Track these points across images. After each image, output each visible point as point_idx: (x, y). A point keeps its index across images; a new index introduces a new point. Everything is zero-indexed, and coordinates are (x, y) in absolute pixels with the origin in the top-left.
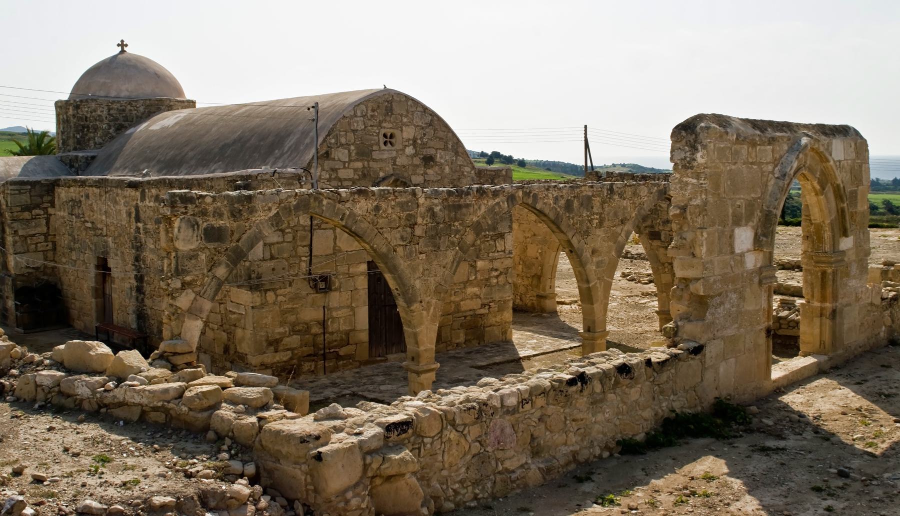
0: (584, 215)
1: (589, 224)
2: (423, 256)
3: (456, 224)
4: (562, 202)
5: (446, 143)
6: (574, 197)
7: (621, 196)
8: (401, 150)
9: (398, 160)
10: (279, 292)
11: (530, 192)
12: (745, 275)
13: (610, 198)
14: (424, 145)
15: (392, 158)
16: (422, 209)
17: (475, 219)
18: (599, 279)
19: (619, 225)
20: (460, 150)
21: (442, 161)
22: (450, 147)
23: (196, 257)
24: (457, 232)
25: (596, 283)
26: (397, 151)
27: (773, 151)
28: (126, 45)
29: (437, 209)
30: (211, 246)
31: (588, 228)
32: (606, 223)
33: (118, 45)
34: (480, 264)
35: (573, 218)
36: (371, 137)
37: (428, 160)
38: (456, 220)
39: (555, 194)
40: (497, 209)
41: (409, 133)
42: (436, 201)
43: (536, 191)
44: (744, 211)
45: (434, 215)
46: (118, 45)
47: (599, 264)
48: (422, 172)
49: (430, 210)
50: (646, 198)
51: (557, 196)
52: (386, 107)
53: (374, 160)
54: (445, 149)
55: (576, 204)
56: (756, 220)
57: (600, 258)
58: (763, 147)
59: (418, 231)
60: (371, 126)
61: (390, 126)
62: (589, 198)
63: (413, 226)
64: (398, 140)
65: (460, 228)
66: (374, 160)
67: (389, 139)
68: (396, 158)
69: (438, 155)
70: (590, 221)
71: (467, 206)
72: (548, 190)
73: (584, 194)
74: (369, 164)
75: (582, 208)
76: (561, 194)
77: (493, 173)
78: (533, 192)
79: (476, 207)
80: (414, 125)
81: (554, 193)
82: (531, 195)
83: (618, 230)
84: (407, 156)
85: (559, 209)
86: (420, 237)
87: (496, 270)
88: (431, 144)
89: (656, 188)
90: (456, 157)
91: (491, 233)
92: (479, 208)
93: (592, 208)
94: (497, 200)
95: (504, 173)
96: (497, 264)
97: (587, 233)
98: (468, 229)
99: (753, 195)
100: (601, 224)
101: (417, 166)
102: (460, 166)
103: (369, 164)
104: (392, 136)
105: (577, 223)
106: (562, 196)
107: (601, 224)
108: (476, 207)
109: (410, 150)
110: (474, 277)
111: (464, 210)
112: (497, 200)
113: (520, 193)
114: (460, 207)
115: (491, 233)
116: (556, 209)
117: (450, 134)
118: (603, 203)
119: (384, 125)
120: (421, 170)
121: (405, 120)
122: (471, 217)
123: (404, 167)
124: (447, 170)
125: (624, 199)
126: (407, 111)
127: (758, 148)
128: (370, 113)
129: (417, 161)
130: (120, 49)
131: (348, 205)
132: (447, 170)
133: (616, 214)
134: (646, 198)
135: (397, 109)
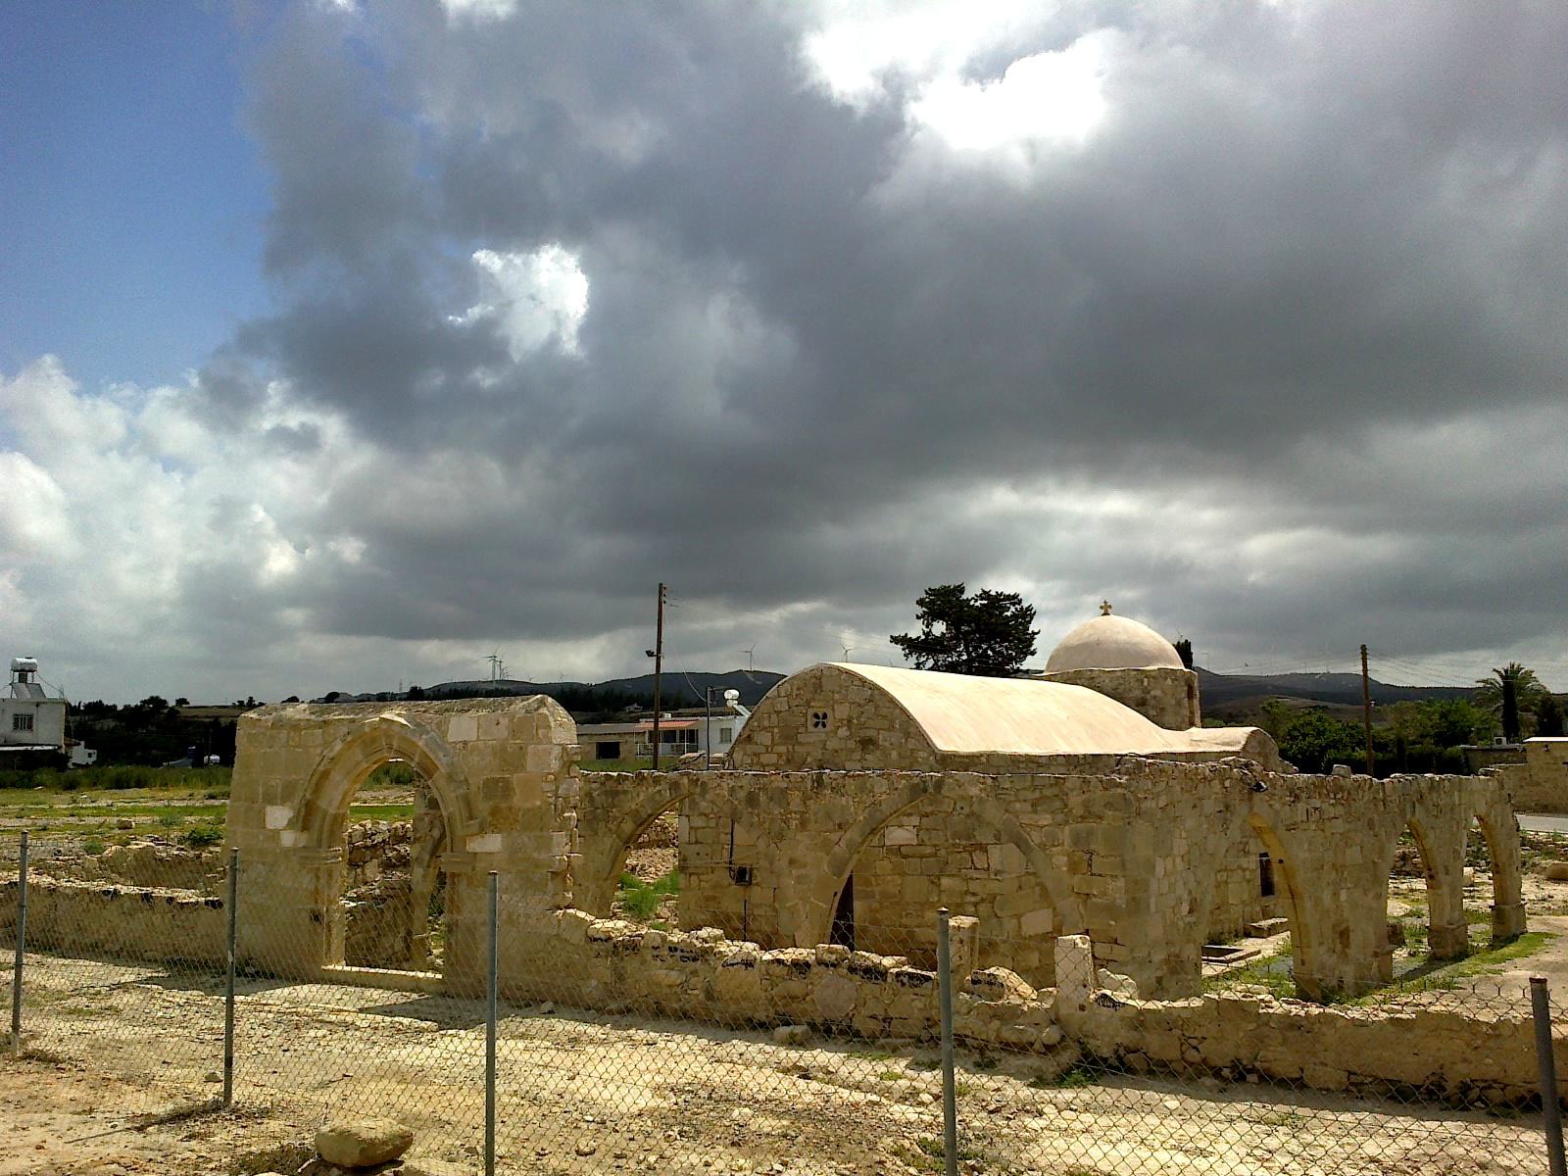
1: (783, 824)
3: (614, 810)
4: (742, 794)
5: (892, 722)
6: (759, 789)
8: (832, 732)
9: (828, 743)
10: (702, 877)
11: (698, 780)
12: (278, 851)
13: (817, 793)
14: (862, 726)
15: (822, 741)
17: (633, 807)
18: (801, 899)
19: (834, 831)
20: (912, 730)
21: (887, 744)
22: (897, 726)
23: (423, 819)
24: (616, 818)
25: (797, 904)
26: (827, 733)
27: (323, 732)
28: (1110, 607)
29: (595, 794)
30: (431, 811)
31: (782, 829)
32: (812, 826)
33: (1101, 607)
34: (945, 882)
35: (758, 815)
36: (796, 718)
37: (867, 744)
38: (614, 806)
39: (732, 784)
40: (657, 797)
41: (842, 711)
42: (594, 786)
43: (706, 779)
44: (280, 790)
46: (1101, 607)
47: (799, 879)
48: (859, 758)
51: (733, 787)
52: (814, 684)
53: (800, 744)
54: (891, 728)
55: (763, 798)
56: (296, 801)
57: (803, 871)
60: (797, 706)
61: (821, 704)
62: (784, 791)
64: (829, 721)
65: (617, 815)
66: (800, 744)
67: (820, 720)
68: (826, 741)
69: (881, 737)
71: (625, 792)
74: (793, 749)
75: (772, 803)
76: (740, 784)
77: (967, 760)
80: (850, 703)
82: (699, 783)
83: (835, 837)
84: (840, 739)
87: (974, 894)
88: (871, 723)
89: (903, 782)
90: (906, 741)
91: (964, 842)
92: (638, 795)
93: (789, 804)
95: (984, 760)
96: (974, 886)
97: (781, 837)
98: (626, 817)
99: (294, 776)
101: (853, 751)
102: (912, 750)
103: (793, 749)
104: (825, 716)
105: (764, 822)
106: (741, 787)
107: (803, 825)
108: (634, 795)
109: (843, 732)
110: (936, 899)
111: (622, 796)
113: (685, 780)
114: (617, 793)
115: (964, 842)
116: (732, 803)
117: (898, 711)
119: (812, 704)
120: (857, 756)
121: (837, 696)
122: (629, 804)
123: (836, 751)
124: (894, 754)
126: (841, 686)
127: (303, 732)
128: (795, 692)
129: (851, 744)
130: (1103, 611)
132: (894, 754)
133: (828, 816)
134: (884, 796)
135: (827, 685)
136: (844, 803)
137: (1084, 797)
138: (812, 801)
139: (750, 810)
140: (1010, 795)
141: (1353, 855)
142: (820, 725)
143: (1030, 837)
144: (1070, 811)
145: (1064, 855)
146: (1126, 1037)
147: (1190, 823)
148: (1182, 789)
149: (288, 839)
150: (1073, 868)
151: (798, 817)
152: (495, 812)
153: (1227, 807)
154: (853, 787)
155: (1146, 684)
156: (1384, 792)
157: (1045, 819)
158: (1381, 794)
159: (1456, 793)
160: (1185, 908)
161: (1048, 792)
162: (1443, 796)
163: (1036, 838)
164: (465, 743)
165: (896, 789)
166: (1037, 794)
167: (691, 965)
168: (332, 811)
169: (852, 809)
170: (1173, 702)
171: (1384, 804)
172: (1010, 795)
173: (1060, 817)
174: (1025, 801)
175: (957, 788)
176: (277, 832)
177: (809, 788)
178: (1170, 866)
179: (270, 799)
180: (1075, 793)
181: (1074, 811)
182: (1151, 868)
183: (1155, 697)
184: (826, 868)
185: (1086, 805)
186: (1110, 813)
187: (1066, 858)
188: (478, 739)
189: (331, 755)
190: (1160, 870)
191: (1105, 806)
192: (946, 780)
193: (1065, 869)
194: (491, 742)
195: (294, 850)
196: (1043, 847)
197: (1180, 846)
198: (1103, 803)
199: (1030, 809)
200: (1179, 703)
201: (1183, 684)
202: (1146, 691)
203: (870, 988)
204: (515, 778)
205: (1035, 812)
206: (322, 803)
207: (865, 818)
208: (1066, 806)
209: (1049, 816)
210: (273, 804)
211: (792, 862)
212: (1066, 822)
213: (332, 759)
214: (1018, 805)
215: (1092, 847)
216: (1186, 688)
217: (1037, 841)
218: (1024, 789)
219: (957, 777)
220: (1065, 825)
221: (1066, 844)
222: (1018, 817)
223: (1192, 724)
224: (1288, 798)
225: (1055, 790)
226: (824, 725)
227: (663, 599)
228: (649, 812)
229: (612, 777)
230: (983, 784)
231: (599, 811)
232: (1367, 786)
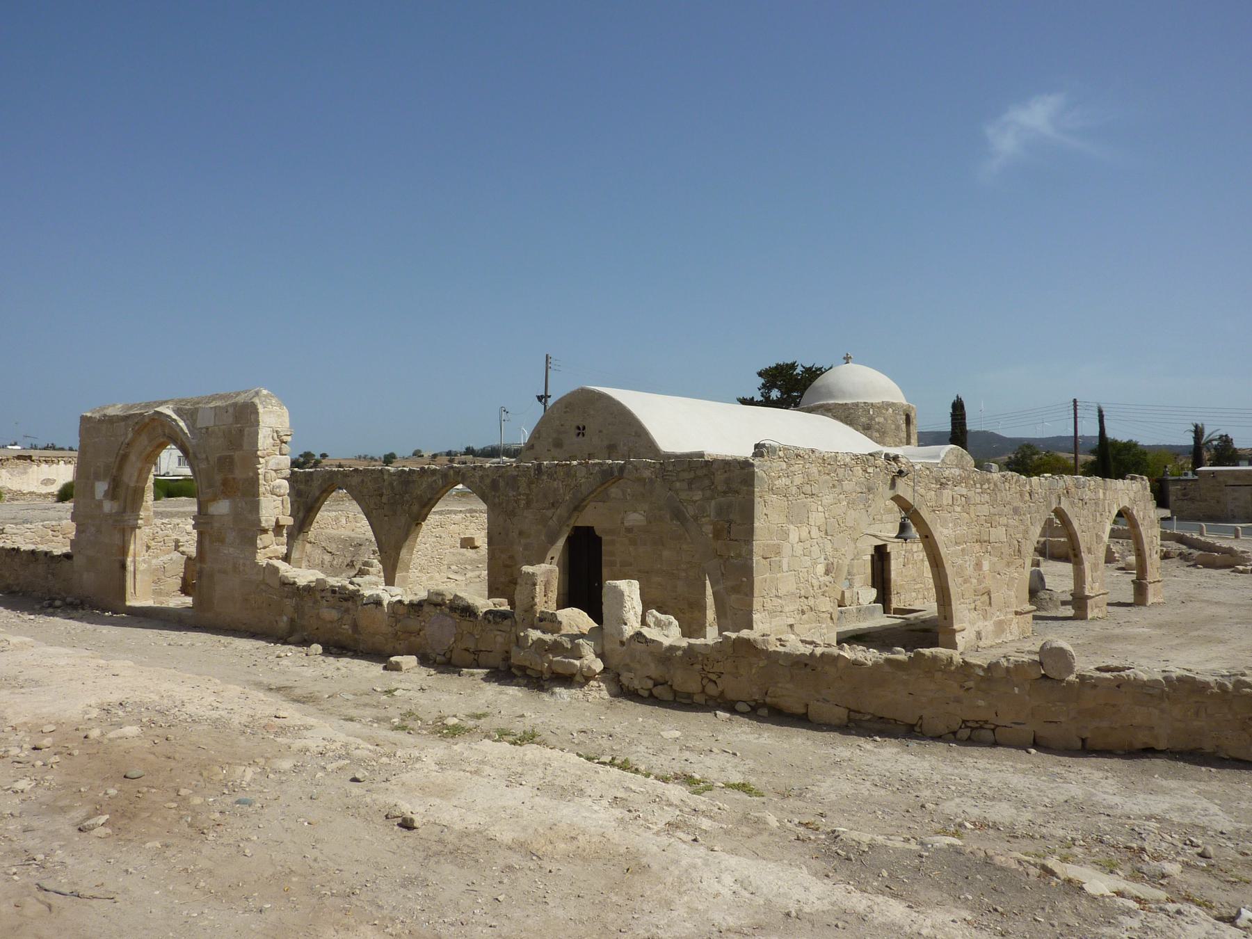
0: (510, 495)
1: (515, 504)
2: (386, 518)
3: (407, 495)
4: (488, 481)
6: (499, 476)
7: (550, 476)
11: (460, 471)
12: (101, 516)
16: (386, 483)
17: (419, 493)
19: (548, 509)
24: (408, 501)
33: (844, 358)
35: (499, 497)
39: (481, 473)
42: (394, 478)
45: (393, 488)
46: (844, 358)
49: (391, 484)
50: (583, 480)
51: (482, 475)
55: (502, 484)
58: (117, 424)
59: (384, 499)
63: (381, 495)
67: (581, 431)
70: (517, 501)
71: (413, 482)
72: (475, 469)
73: (510, 473)
78: (462, 472)
79: (420, 483)
81: (480, 472)
83: (549, 513)
85: (484, 488)
86: (385, 504)
93: (518, 488)
94: (434, 478)
100: (528, 504)
104: (584, 428)
105: (502, 503)
107: (528, 504)
112: (434, 478)
116: (482, 488)
118: (530, 483)
125: (555, 480)
127: (115, 425)
130: (845, 361)
131: (349, 478)
134: (583, 480)
136: (556, 486)
137: (726, 475)
138: (534, 485)
139: (493, 493)
140: (672, 476)
141: (999, 534)
142: (581, 435)
143: (687, 510)
144: (716, 487)
145: (711, 525)
146: (654, 670)
147: (828, 499)
148: (819, 471)
149: (108, 506)
150: (717, 535)
151: (525, 498)
152: (225, 483)
153: (870, 489)
154: (562, 473)
155: (871, 413)
156: (1031, 486)
157: (698, 496)
158: (1028, 487)
159: (1101, 491)
160: (821, 569)
161: (700, 473)
162: (1089, 492)
163: (690, 511)
164: (207, 428)
165: (592, 474)
166: (692, 475)
167: (345, 604)
168: (132, 484)
169: (561, 491)
170: (893, 426)
171: (1030, 495)
172: (672, 476)
173: (708, 493)
174: (684, 480)
175: (635, 471)
176: (101, 502)
177: (532, 475)
178: (804, 534)
179: (97, 477)
180: (719, 473)
181: (719, 488)
182: (785, 535)
183: (879, 423)
184: (543, 538)
185: (728, 481)
186: (745, 488)
187: (712, 527)
188: (214, 426)
189: (126, 441)
190: (794, 537)
191: (741, 482)
192: (628, 466)
193: (711, 535)
194: (222, 427)
195: (110, 515)
196: (696, 518)
197: (817, 517)
198: (739, 481)
199: (687, 487)
200: (898, 428)
201: (902, 413)
202: (871, 419)
203: (466, 625)
204: (237, 455)
205: (690, 489)
206: (125, 478)
207: (570, 497)
208: (713, 483)
209: (700, 492)
210: (99, 480)
211: (521, 533)
212: (713, 498)
213: (128, 444)
214: (678, 484)
215: (731, 517)
216: (904, 417)
217: (692, 513)
218: (683, 470)
219: (635, 463)
220: (712, 499)
221: (712, 514)
222: (678, 494)
223: (908, 443)
224: (934, 486)
225: (705, 471)
226: (583, 435)
227: (549, 365)
228: (429, 497)
229: (405, 471)
230: (654, 467)
231: (398, 496)
232: (1014, 480)
